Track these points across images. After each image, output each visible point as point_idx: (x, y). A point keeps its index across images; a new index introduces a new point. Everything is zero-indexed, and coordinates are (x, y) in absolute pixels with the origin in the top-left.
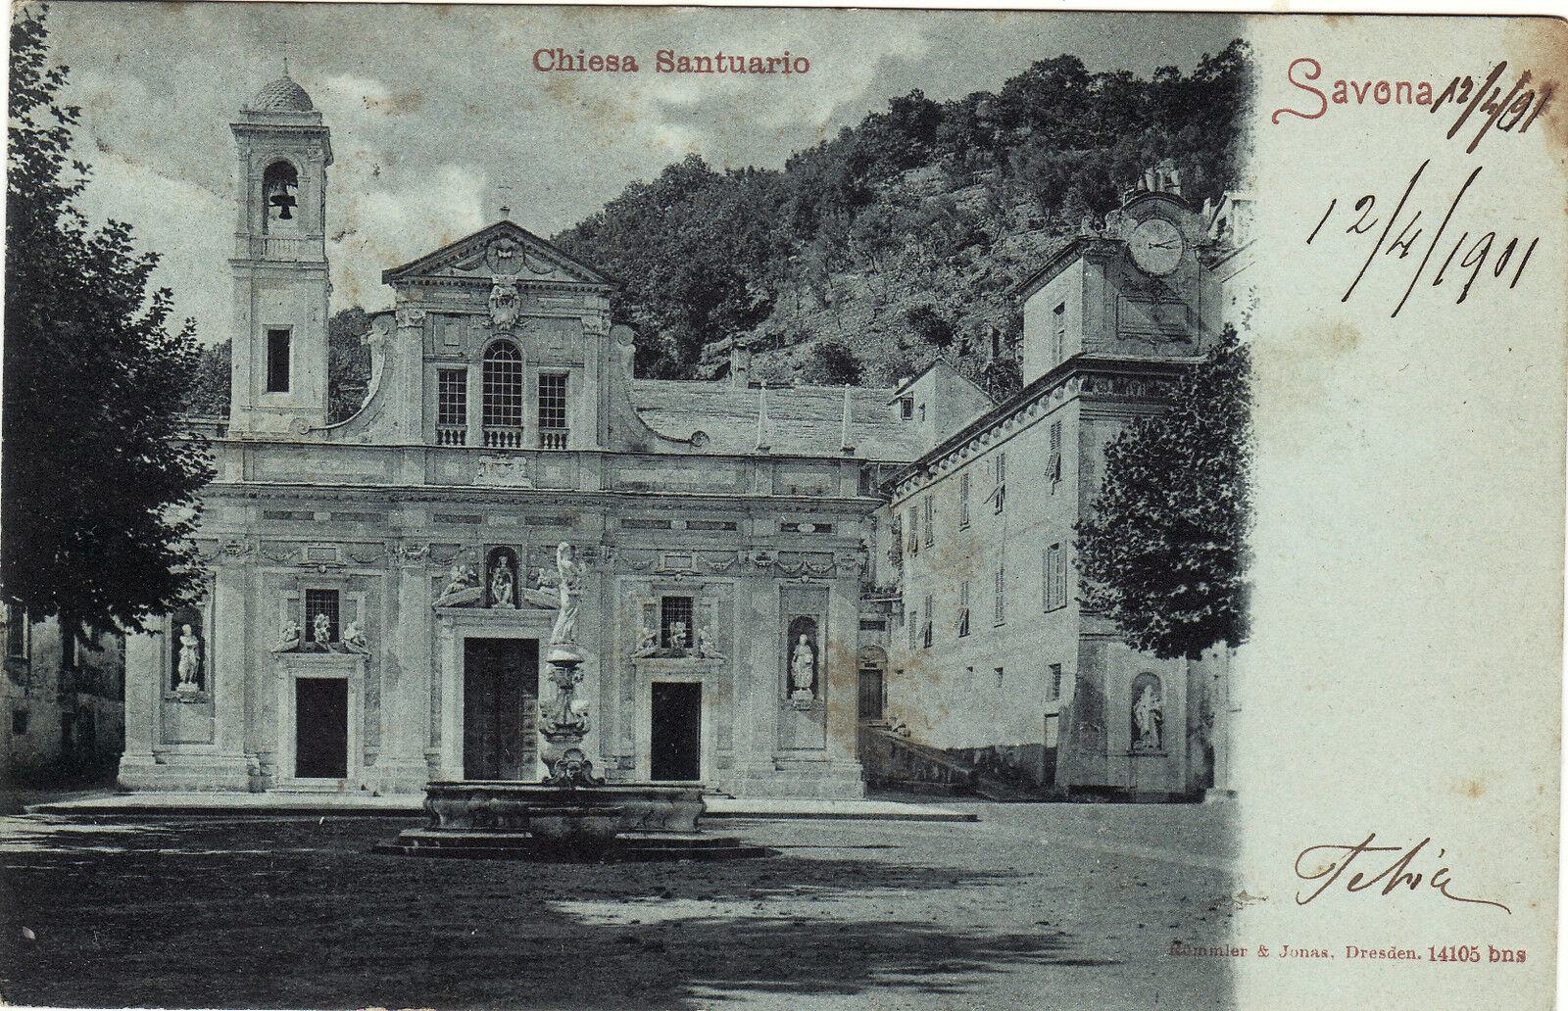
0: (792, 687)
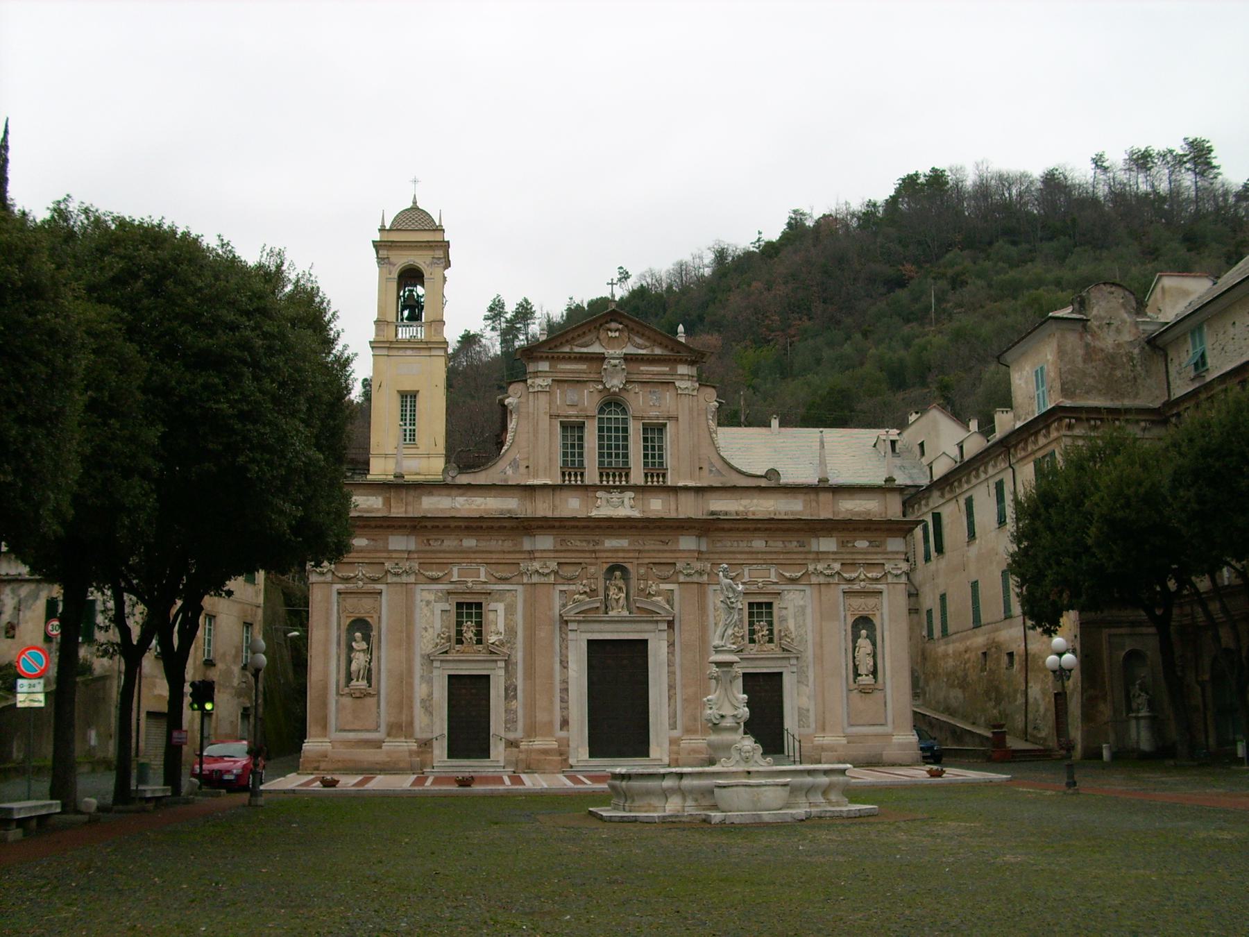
0: (857, 674)
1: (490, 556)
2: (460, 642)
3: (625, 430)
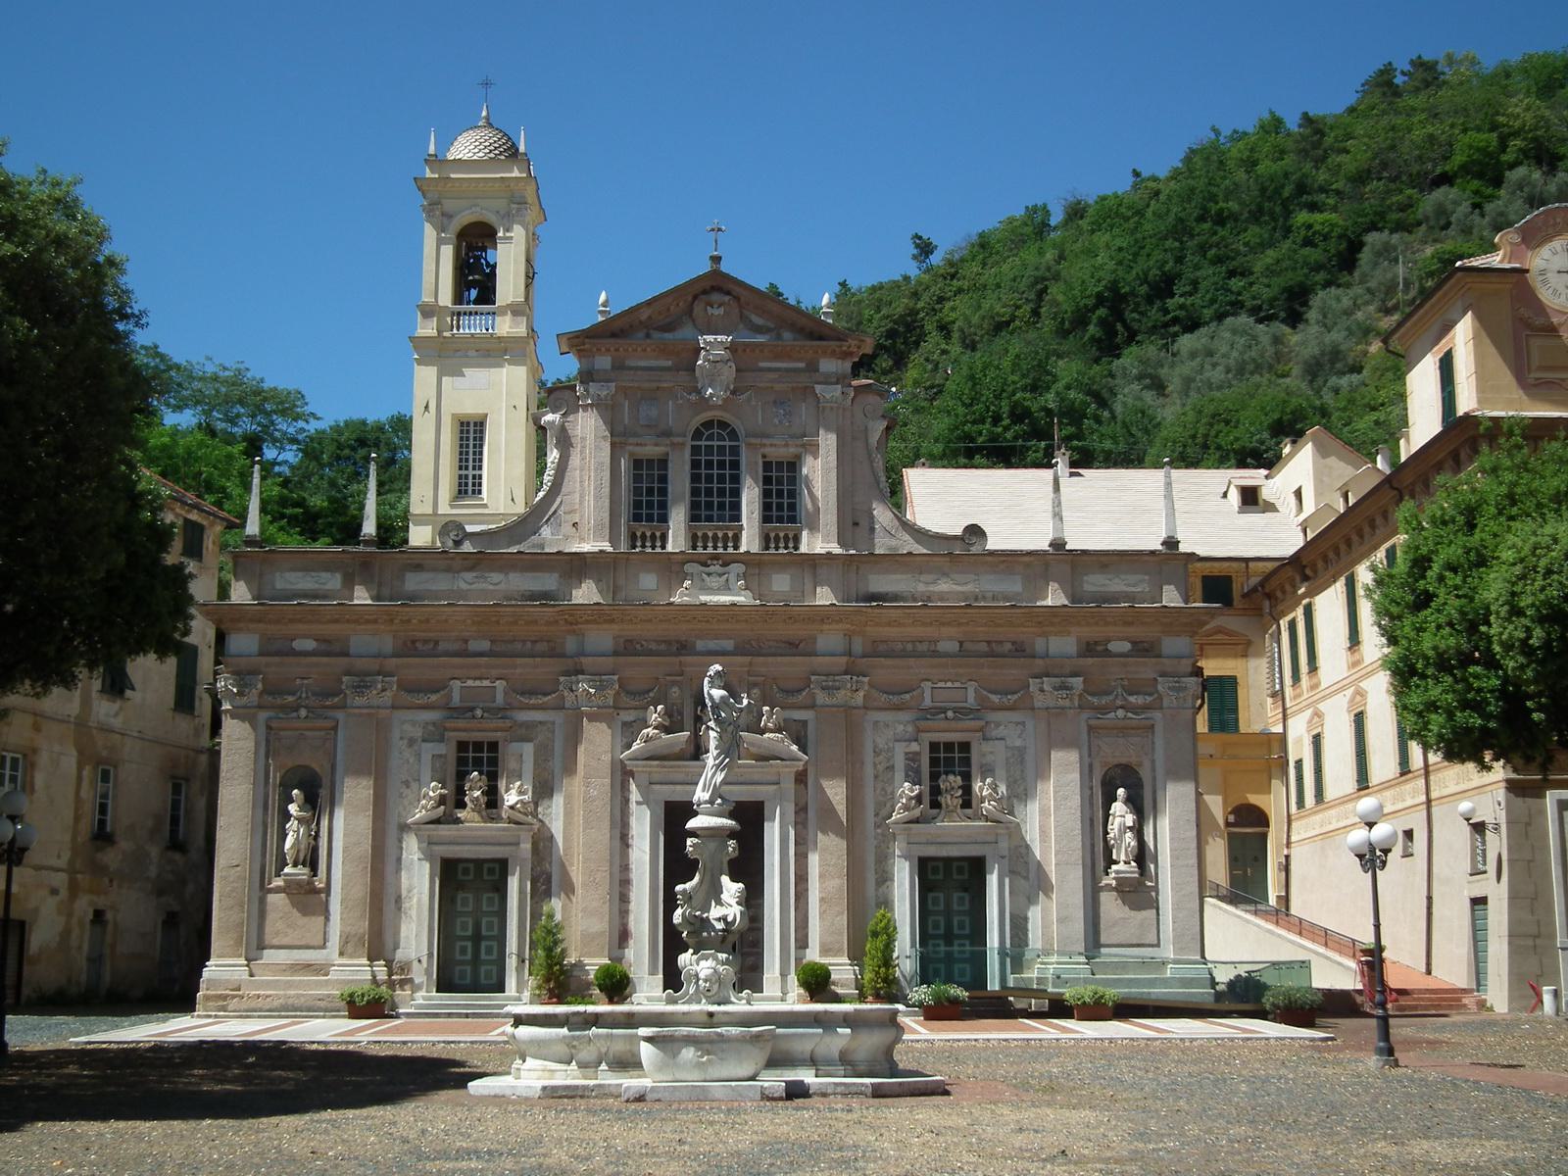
3: (735, 465)
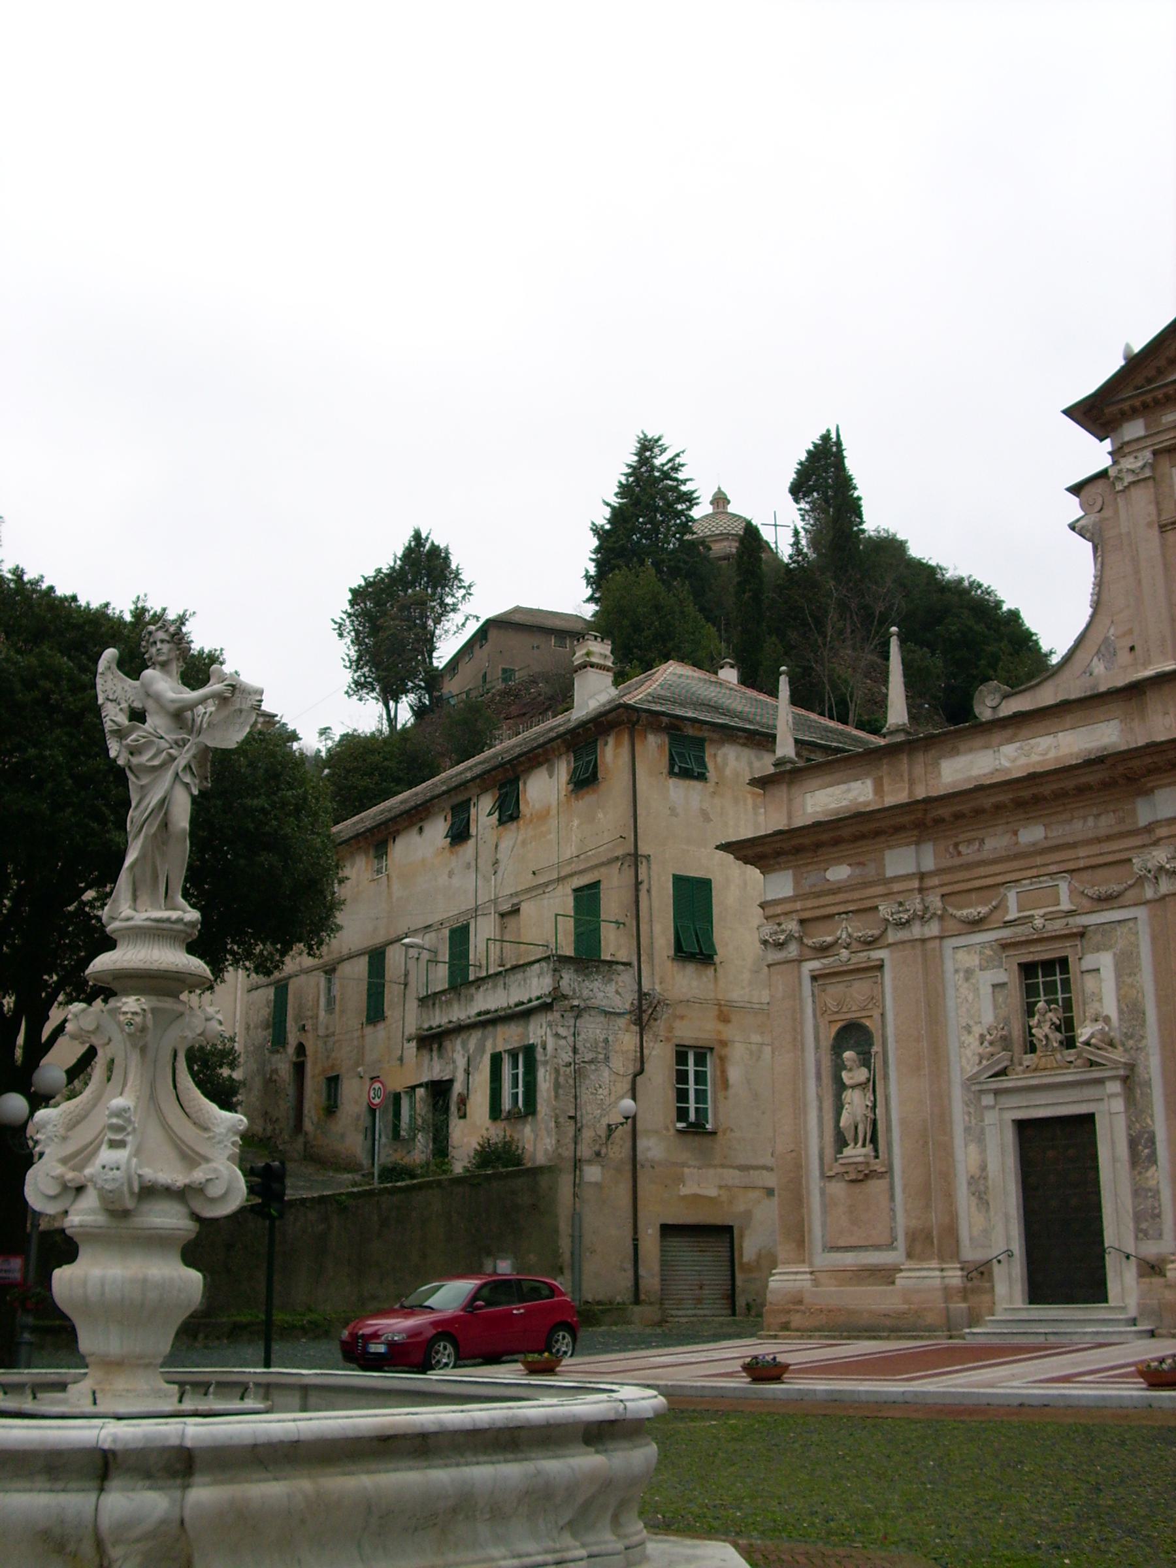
1: (1070, 854)
2: (1033, 1049)
